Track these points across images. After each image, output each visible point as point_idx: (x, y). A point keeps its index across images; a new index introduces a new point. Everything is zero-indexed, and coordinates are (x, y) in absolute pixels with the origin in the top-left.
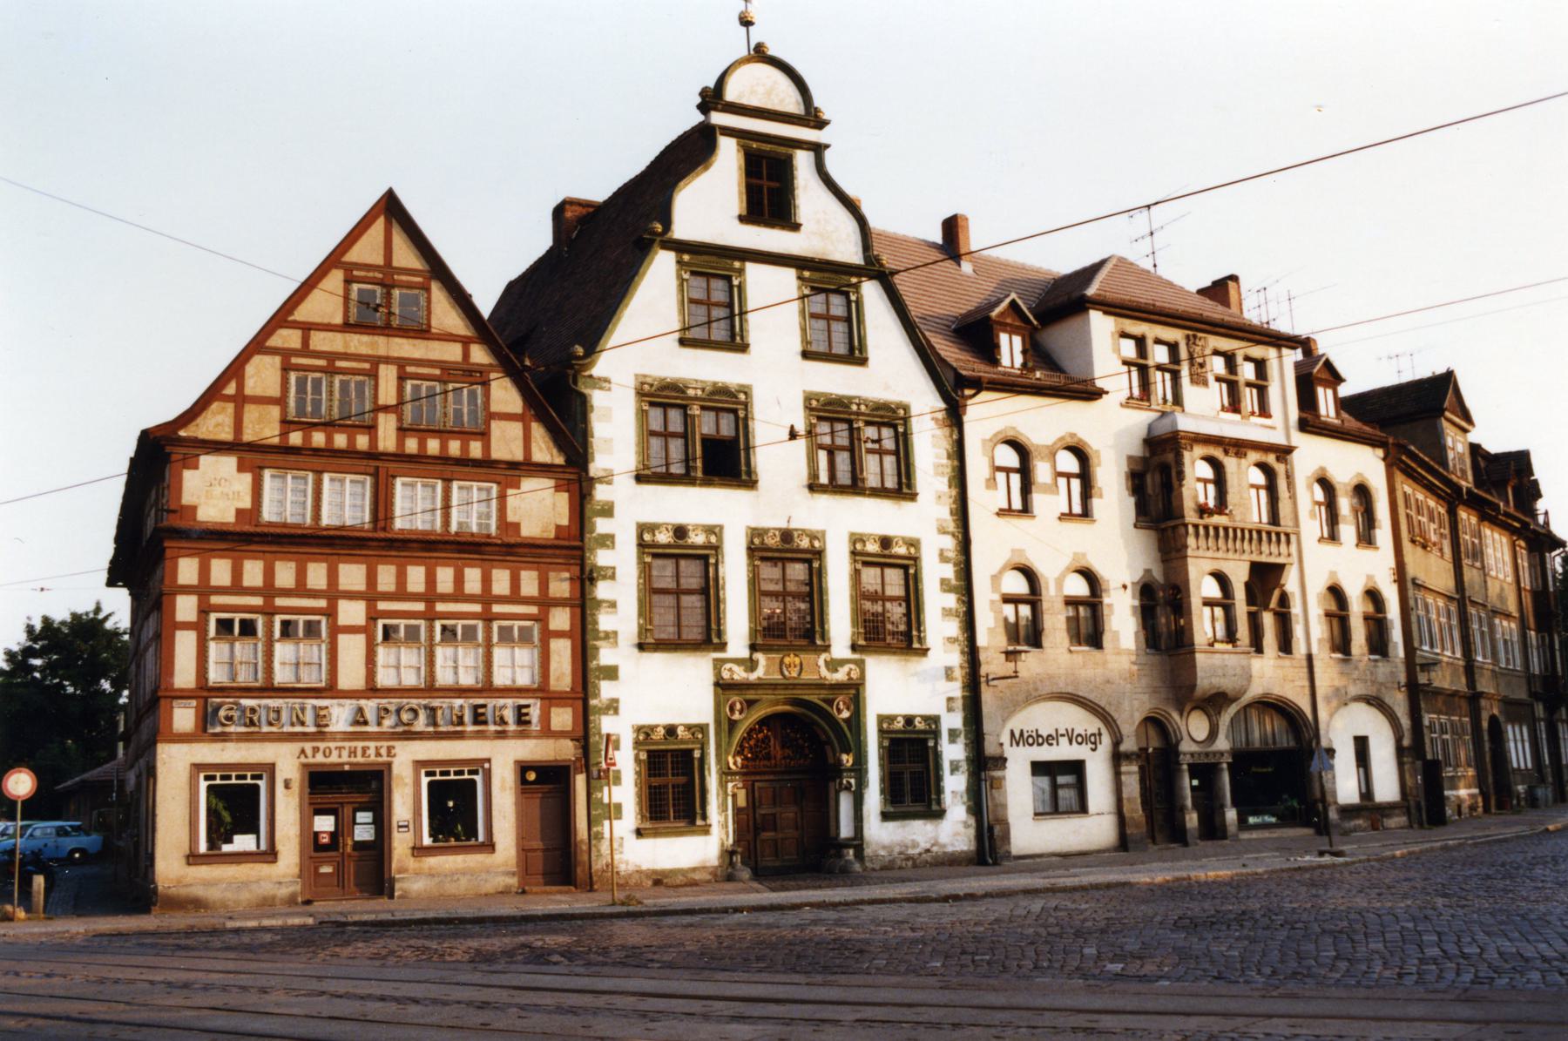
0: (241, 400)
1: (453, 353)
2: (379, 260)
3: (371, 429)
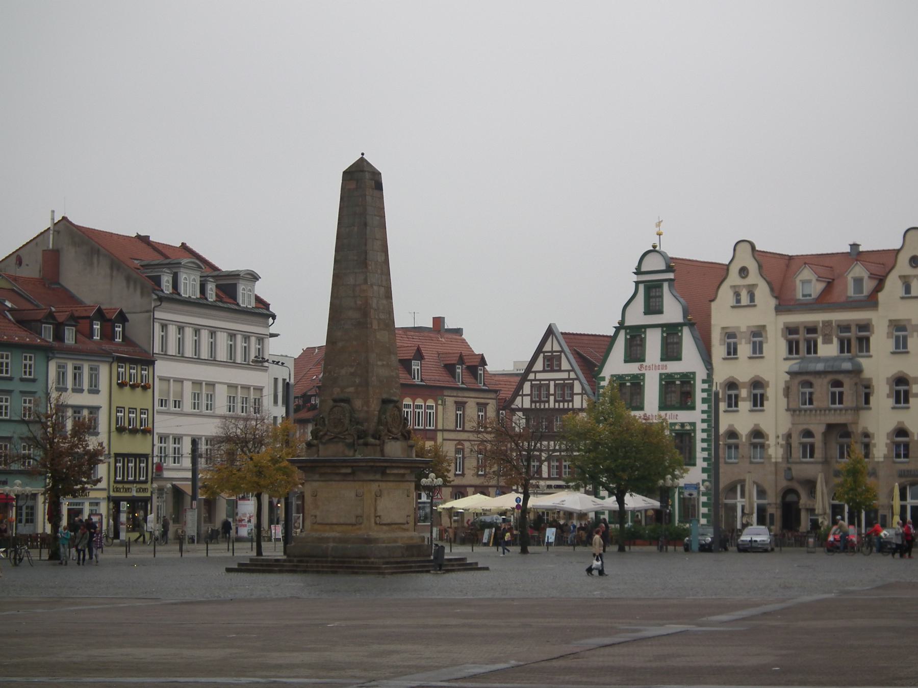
0: (523, 395)
1: (564, 375)
2: (550, 349)
3: (548, 401)
